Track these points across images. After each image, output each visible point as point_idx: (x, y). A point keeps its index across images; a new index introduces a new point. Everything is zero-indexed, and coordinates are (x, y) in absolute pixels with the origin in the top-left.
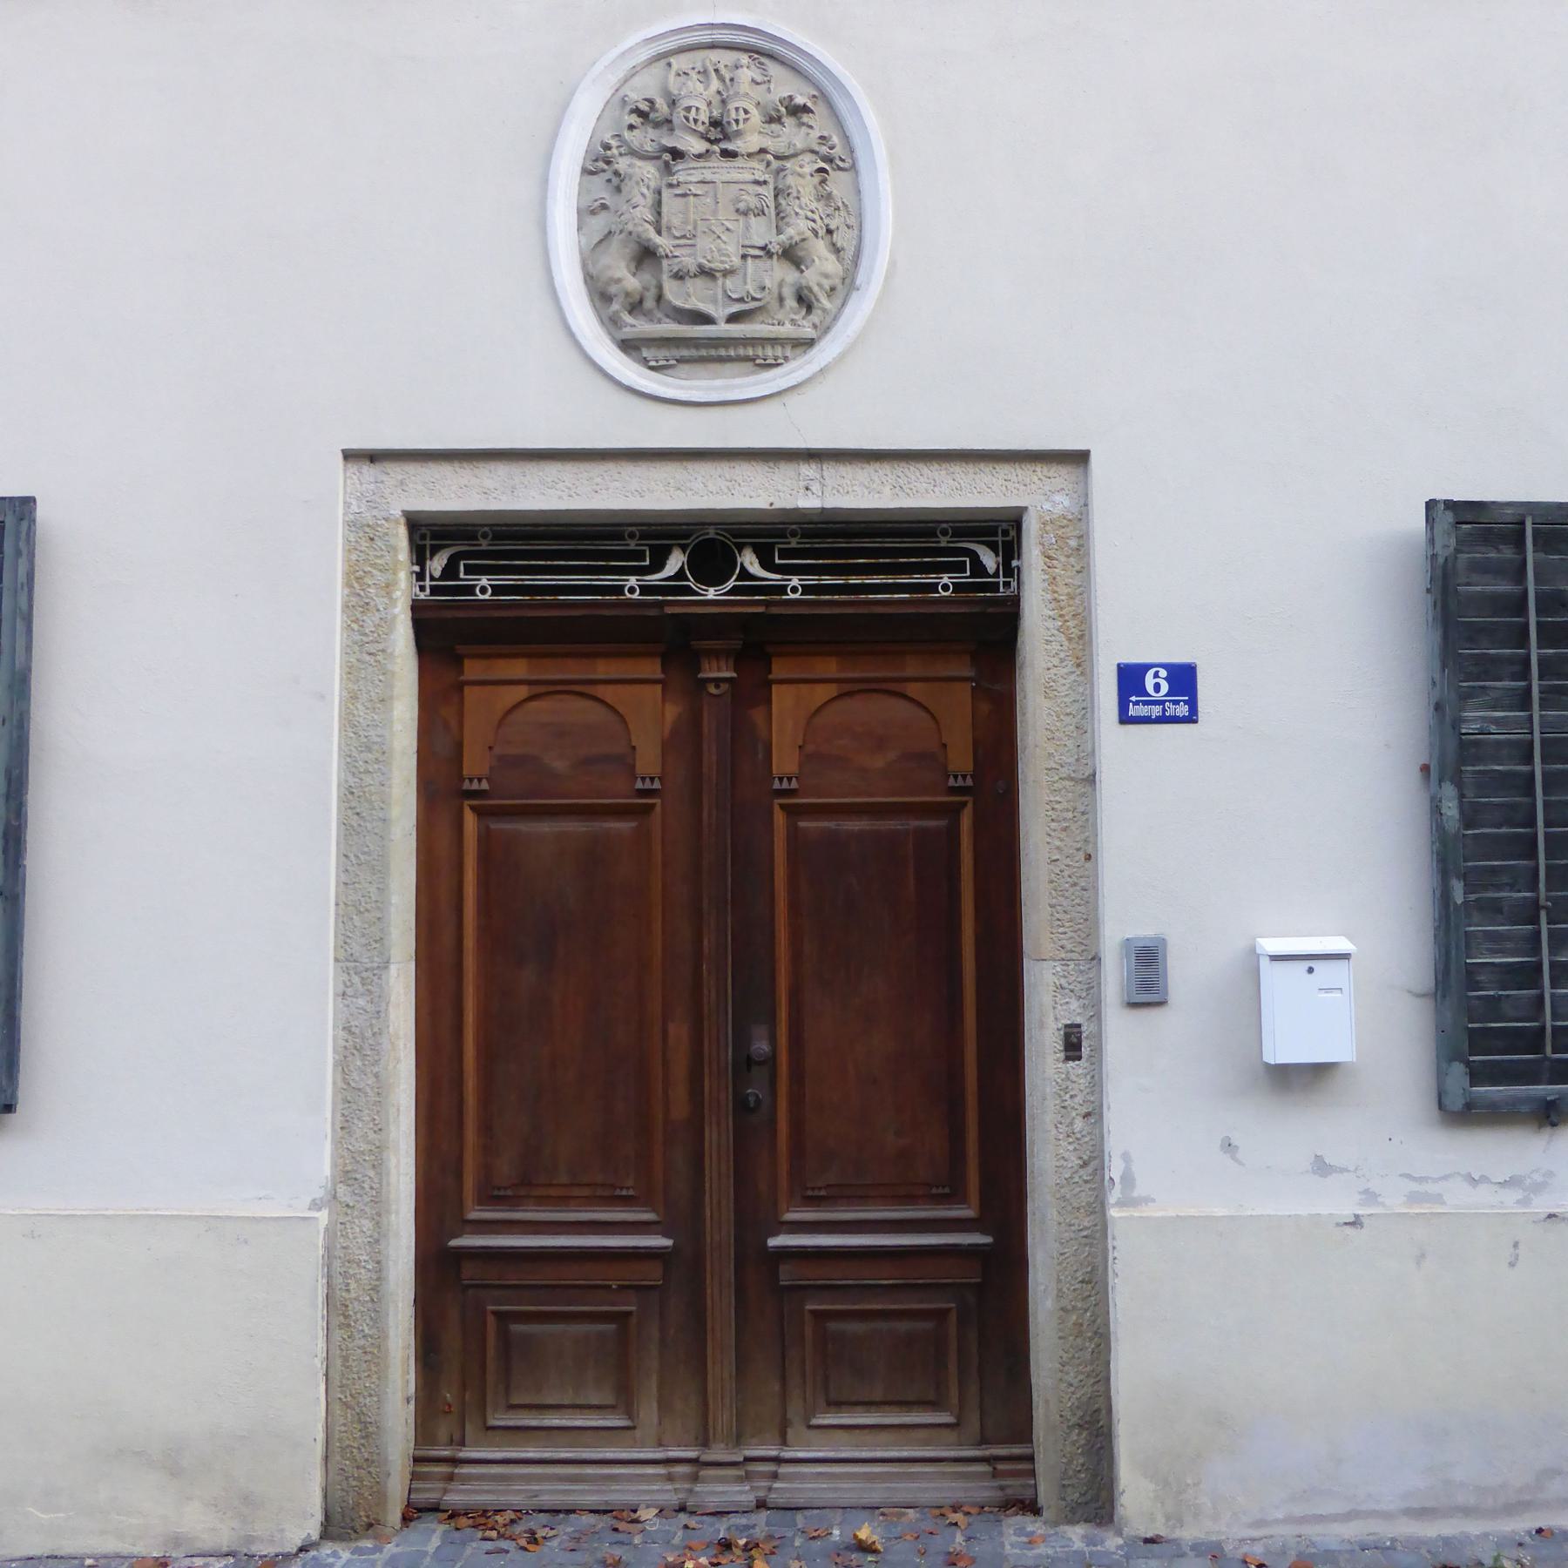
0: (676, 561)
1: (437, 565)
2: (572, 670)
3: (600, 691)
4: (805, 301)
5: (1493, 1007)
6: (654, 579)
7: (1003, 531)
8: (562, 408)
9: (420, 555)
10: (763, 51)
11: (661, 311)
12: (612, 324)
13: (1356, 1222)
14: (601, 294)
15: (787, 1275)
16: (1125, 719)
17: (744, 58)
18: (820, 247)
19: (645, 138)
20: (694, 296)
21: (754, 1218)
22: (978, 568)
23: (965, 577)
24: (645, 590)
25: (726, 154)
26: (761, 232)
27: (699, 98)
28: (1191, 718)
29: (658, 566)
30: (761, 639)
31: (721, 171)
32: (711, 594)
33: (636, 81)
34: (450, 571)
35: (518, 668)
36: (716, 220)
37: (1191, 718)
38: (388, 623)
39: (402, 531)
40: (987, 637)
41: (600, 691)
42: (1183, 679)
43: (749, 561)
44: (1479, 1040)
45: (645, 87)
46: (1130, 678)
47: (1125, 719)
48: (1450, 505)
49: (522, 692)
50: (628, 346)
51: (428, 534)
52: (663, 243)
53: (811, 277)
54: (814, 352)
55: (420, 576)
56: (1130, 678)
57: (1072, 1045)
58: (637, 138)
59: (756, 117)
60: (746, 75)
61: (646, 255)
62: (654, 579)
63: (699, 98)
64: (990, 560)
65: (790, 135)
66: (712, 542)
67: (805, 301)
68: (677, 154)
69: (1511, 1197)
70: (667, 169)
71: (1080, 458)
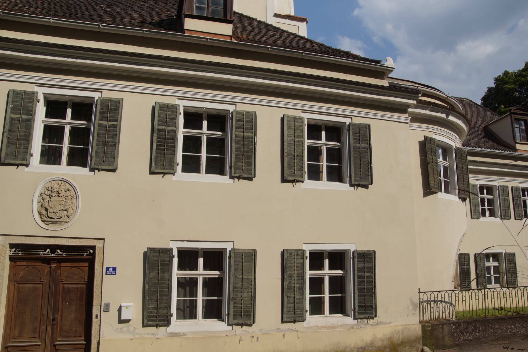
0: (48, 250)
1: (13, 250)
2: (33, 264)
3: (37, 267)
4: (68, 216)
5: (151, 312)
6: (45, 253)
7: (94, 248)
8: (32, 229)
9: (11, 248)
10: (66, 181)
11: (48, 217)
12: (41, 218)
13: (132, 339)
14: (40, 213)
15: (57, 347)
16: (106, 274)
17: (62, 182)
18: (71, 210)
19: (48, 193)
20: (52, 215)
21: (53, 340)
22: (90, 252)
23: (88, 254)
24: (44, 254)
25: (59, 196)
26: (62, 207)
27: (56, 188)
28: (115, 274)
29: (45, 251)
30: (59, 261)
31: (57, 198)
32: (53, 255)
33: (48, 184)
34: (15, 251)
35: (25, 263)
36: (56, 206)
37: (115, 274)
38: (5, 259)
39: (8, 245)
40: (91, 262)
41: (37, 267)
42: (114, 269)
43: (58, 251)
44: (149, 316)
45: (49, 185)
46: (108, 269)
47: (106, 274)
48: (150, 248)
49: (25, 267)
50: (43, 221)
51: (12, 246)
52: (48, 208)
53: (69, 214)
54: (68, 223)
55: (11, 251)
56: (108, 269)
57: (97, 317)
58: (46, 193)
59: (63, 191)
60: (63, 184)
61: (46, 210)
62: (45, 253)
63: (56, 188)
64: (91, 251)
65: (68, 193)
66: (53, 248)
67: (68, 216)
68: (52, 196)
69: (153, 336)
70: (50, 197)
71: (104, 239)
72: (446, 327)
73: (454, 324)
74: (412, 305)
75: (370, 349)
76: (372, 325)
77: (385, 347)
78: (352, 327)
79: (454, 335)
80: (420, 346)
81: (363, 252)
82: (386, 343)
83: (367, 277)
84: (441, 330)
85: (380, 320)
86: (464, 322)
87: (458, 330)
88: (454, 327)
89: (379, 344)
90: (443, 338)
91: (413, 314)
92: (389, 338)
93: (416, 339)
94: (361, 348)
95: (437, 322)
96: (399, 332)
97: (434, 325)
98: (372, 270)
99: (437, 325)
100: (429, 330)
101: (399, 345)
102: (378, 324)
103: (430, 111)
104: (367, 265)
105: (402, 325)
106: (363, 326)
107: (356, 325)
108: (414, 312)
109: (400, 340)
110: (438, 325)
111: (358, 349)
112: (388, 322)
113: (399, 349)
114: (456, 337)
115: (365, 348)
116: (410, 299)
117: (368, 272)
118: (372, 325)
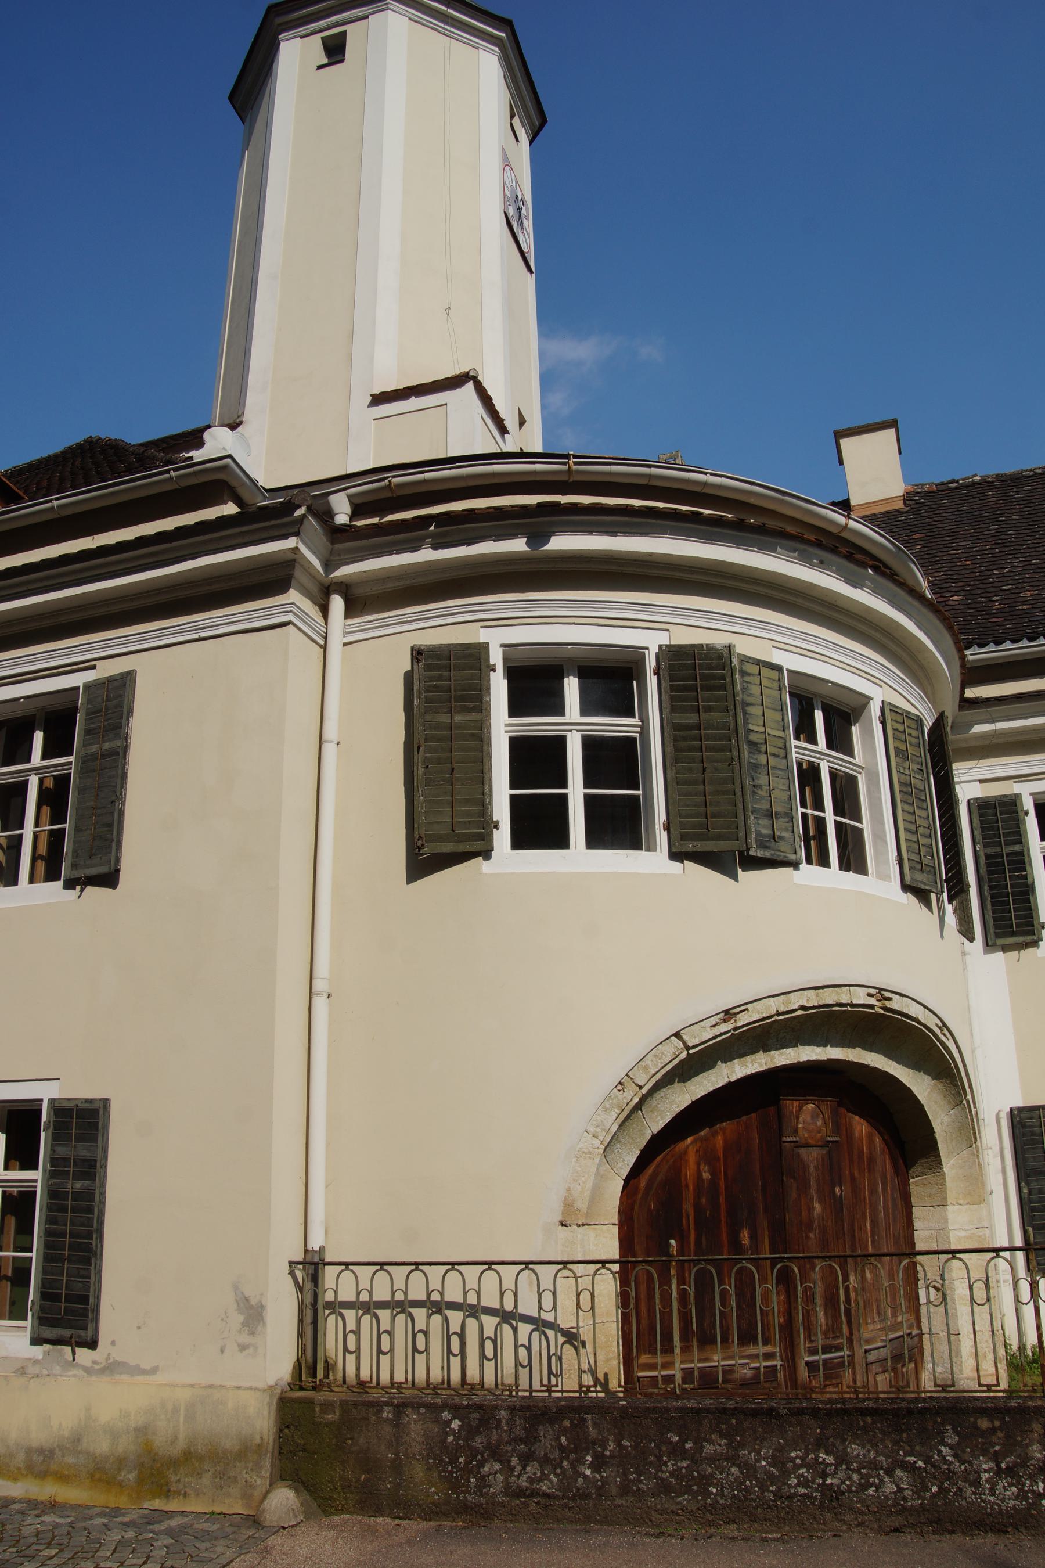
72: (411, 1417)
73: (457, 1411)
74: (239, 1310)
75: (70, 1460)
76: (88, 1371)
77: (121, 1462)
78: (22, 1371)
79: (454, 1461)
80: (260, 1482)
81: (72, 1105)
82: (126, 1445)
83: (77, 1195)
84: (387, 1430)
85: (117, 1355)
86: (512, 1409)
87: (478, 1442)
88: (456, 1424)
89: (102, 1446)
90: (397, 1467)
91: (243, 1348)
92: (137, 1430)
93: (247, 1451)
94: (41, 1451)
95: (375, 1395)
96: (176, 1410)
97: (355, 1405)
98: (92, 1169)
99: (371, 1404)
100: (328, 1424)
101: (174, 1463)
102: (111, 1368)
103: (435, 547)
104: (83, 1152)
105: (192, 1386)
106: (57, 1370)
107: (36, 1362)
108: (245, 1338)
109: (181, 1444)
110: (377, 1406)
111: (29, 1451)
112: (146, 1365)
113: (173, 1478)
114: (467, 1471)
115: (52, 1452)
116: (236, 1288)
117: (78, 1176)
118: (88, 1371)
